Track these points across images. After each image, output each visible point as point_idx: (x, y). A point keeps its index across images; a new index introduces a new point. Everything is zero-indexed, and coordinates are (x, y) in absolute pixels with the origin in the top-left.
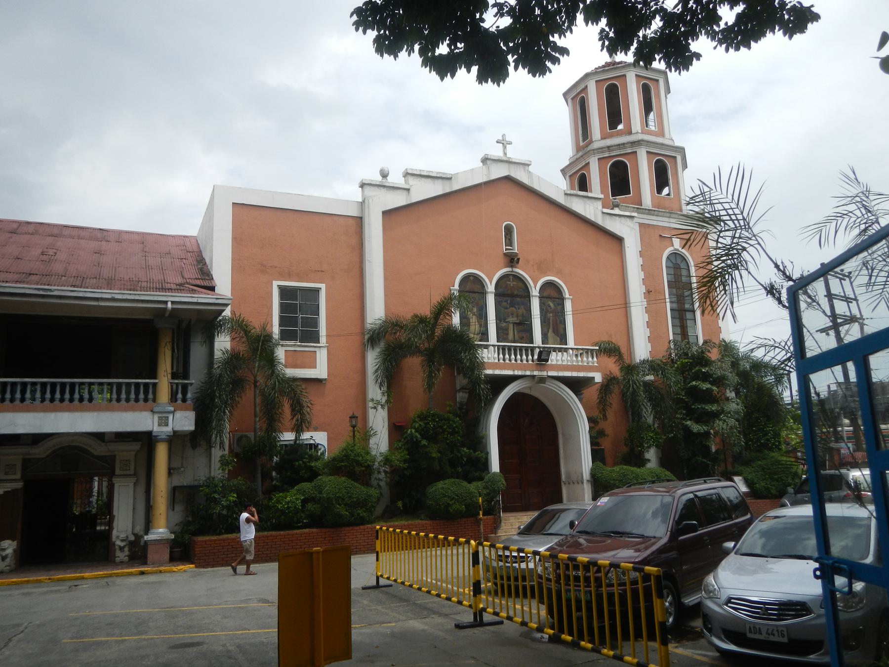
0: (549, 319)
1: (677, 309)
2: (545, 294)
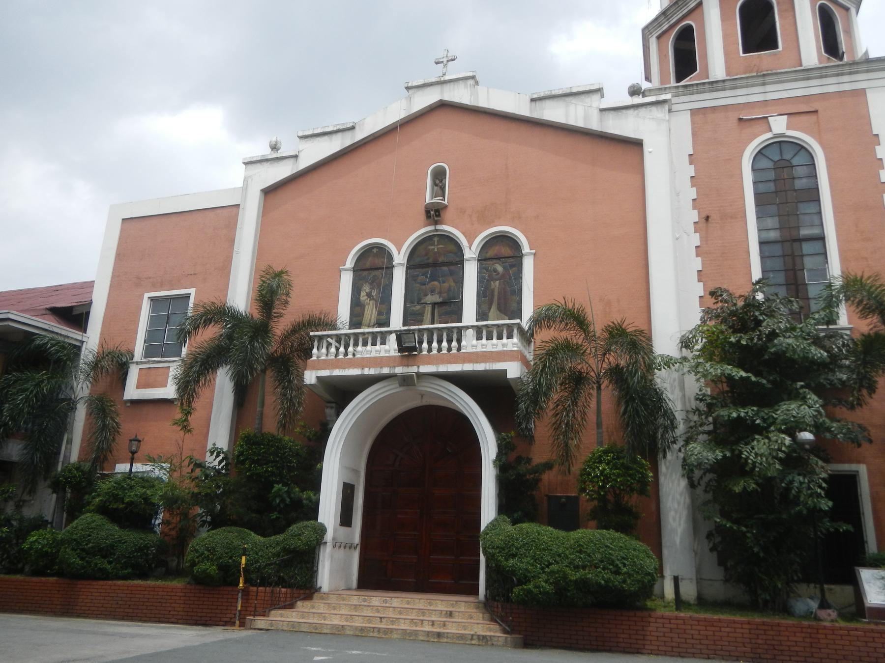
0: (493, 291)
1: (779, 239)
2: (491, 253)
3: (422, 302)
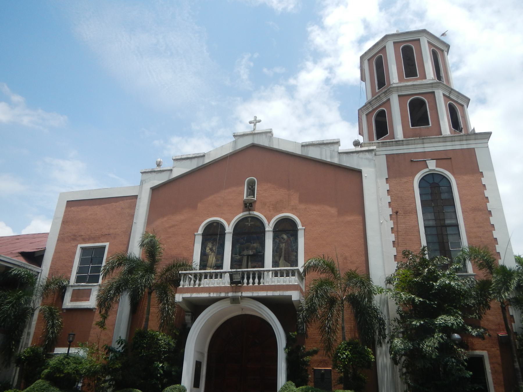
0: (281, 249)
3: (242, 254)
